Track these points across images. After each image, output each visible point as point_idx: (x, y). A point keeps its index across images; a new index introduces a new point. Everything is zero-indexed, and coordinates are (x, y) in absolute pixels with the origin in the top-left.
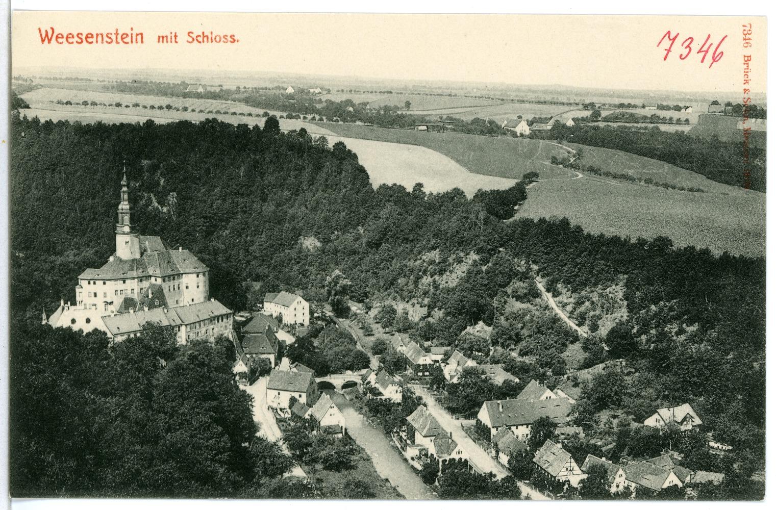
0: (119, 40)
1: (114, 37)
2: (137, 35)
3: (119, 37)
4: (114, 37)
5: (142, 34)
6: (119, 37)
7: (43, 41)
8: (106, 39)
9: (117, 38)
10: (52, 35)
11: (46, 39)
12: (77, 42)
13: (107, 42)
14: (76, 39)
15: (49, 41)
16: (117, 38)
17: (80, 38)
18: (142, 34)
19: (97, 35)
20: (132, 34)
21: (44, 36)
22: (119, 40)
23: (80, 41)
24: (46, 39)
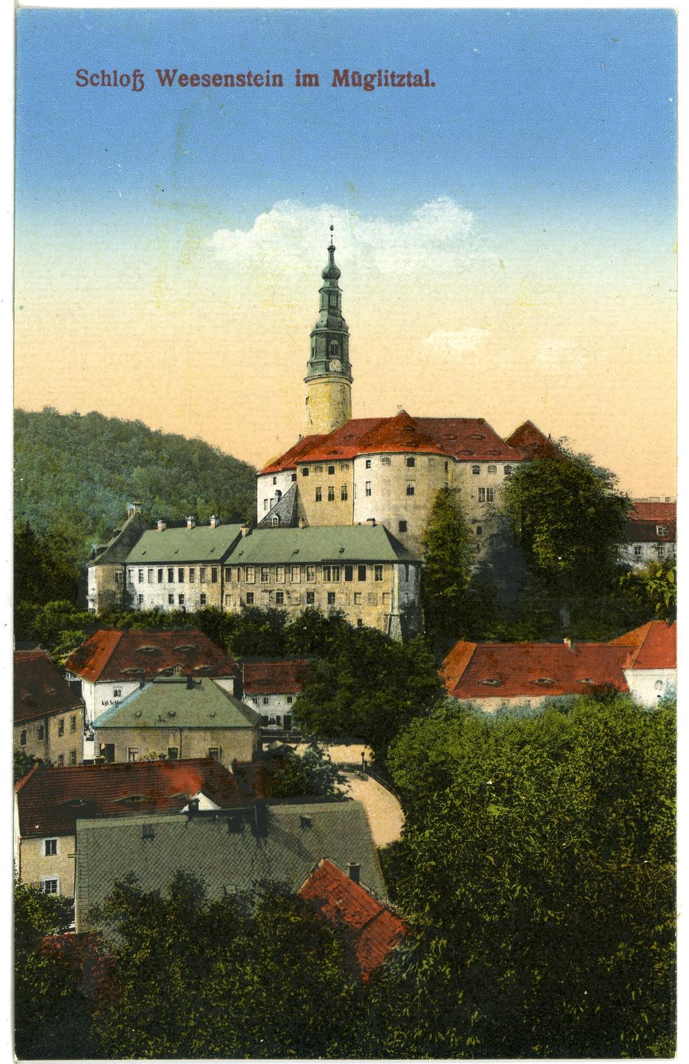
0: (252, 82)
1: (246, 80)
2: (274, 77)
3: (252, 79)
4: (246, 80)
5: (280, 76)
6: (252, 79)
7: (163, 82)
8: (235, 80)
9: (249, 80)
10: (174, 76)
11: (167, 80)
12: (203, 85)
13: (238, 85)
14: (201, 81)
15: (170, 84)
16: (249, 80)
17: (207, 80)
18: (280, 76)
19: (226, 77)
20: (268, 77)
21: (163, 74)
22: (252, 82)
23: (206, 83)
24: (167, 80)
